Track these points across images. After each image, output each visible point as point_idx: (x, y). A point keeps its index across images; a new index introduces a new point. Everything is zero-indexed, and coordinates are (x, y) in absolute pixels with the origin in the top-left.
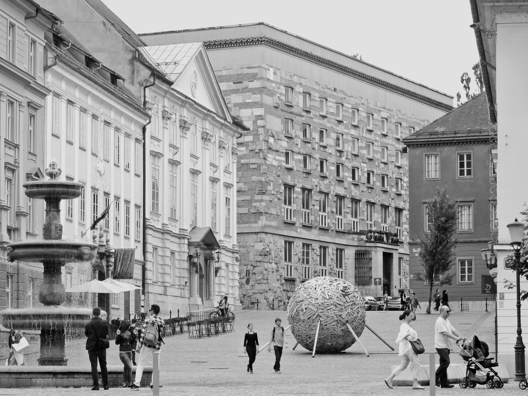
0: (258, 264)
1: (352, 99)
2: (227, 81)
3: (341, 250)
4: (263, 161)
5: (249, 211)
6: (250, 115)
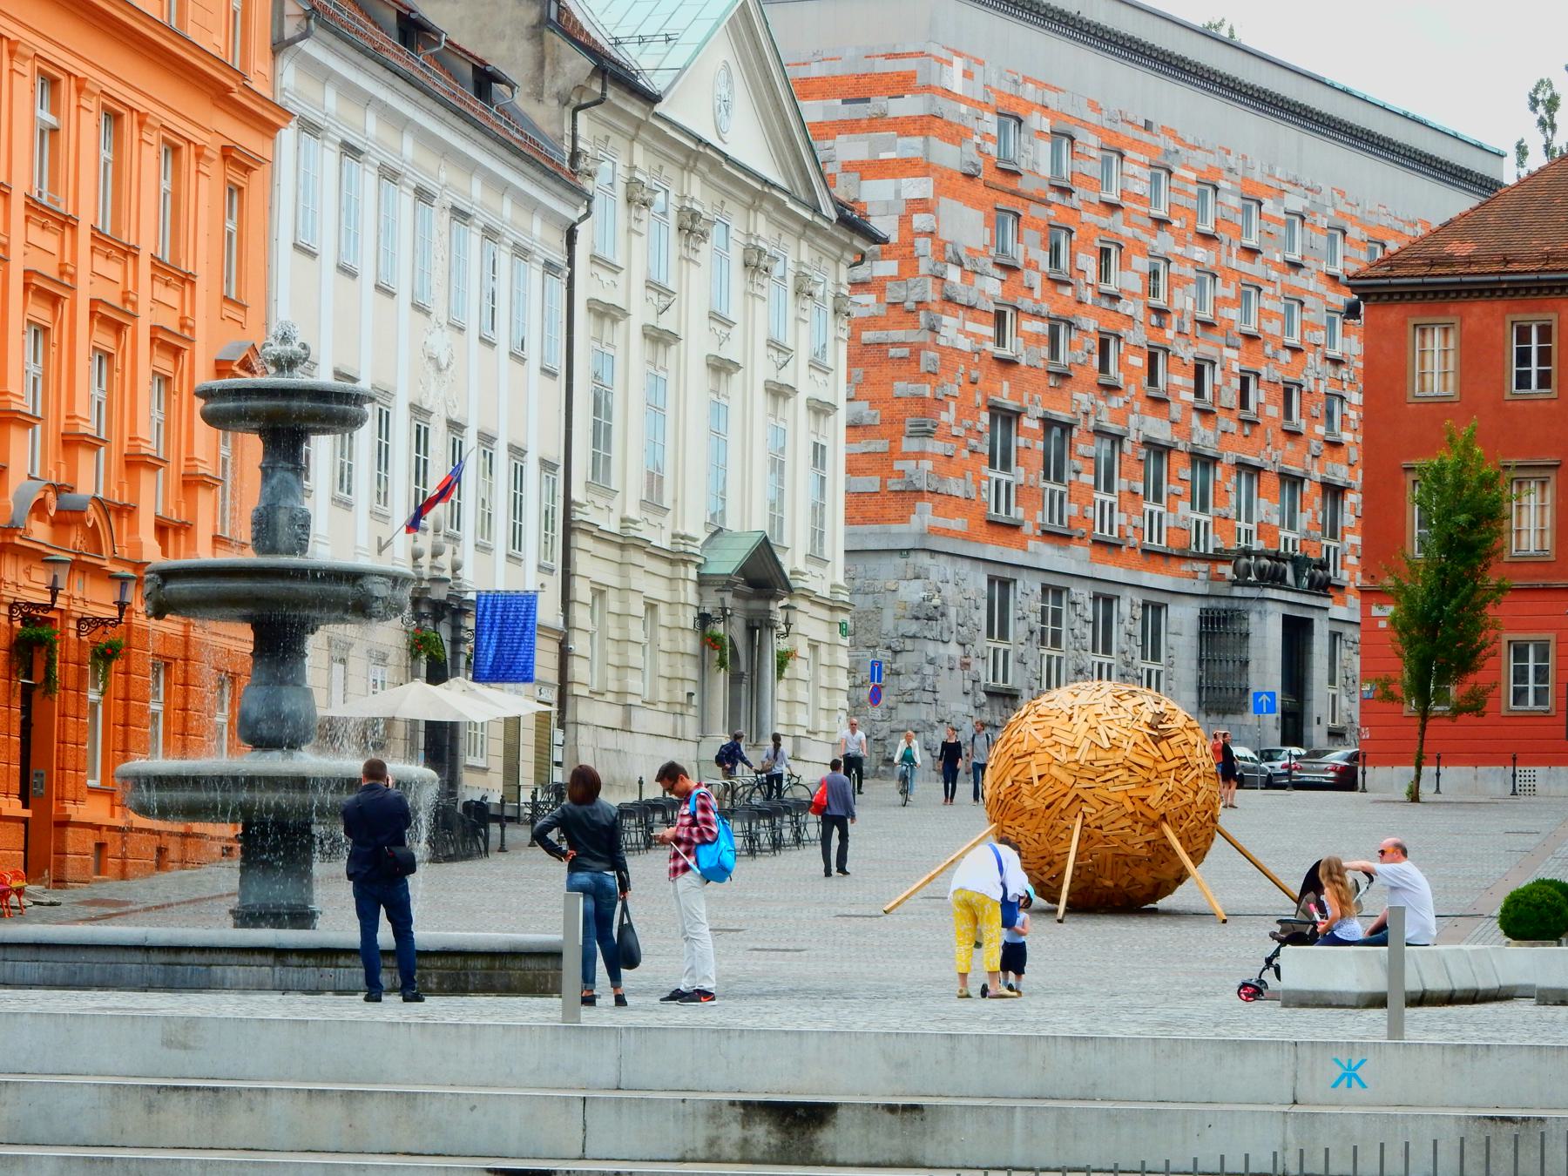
0: (909, 644)
1: (1199, 155)
2: (825, 96)
3: (1158, 608)
4: (925, 337)
5: (883, 484)
6: (891, 197)
